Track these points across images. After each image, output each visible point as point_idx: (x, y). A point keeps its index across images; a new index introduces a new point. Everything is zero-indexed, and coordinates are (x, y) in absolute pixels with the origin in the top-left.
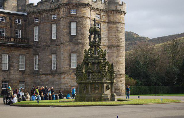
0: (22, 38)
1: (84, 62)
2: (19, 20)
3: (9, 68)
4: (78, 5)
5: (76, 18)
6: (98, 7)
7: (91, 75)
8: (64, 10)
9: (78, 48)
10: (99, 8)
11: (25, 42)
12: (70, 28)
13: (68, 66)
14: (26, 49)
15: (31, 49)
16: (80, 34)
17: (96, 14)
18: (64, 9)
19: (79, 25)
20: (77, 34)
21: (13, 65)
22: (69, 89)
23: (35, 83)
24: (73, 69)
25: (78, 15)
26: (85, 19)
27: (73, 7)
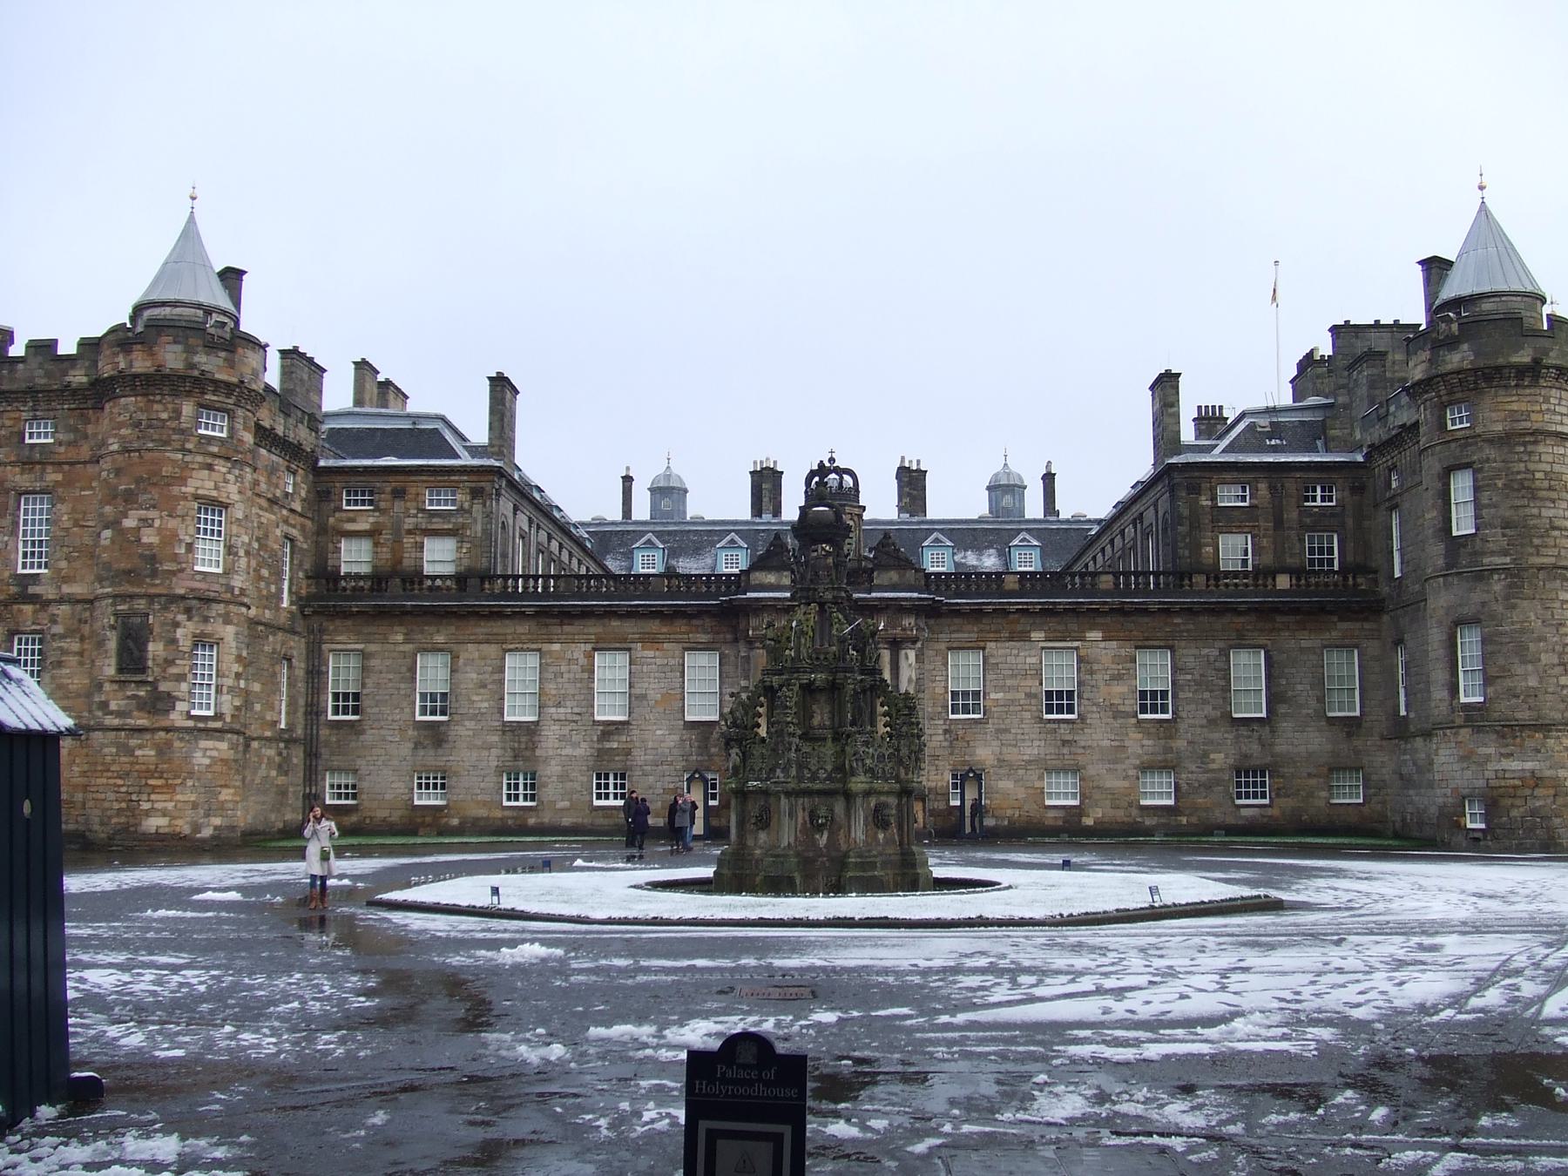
0: (1344, 570)
1: (762, 681)
2: (1323, 490)
3: (1268, 711)
5: (1467, 445)
9: (1486, 597)
11: (1308, 585)
12: (1447, 503)
13: (1445, 694)
14: (1366, 619)
15: (1386, 618)
16: (1492, 526)
19: (1483, 479)
20: (1477, 529)
21: (1290, 693)
23: (1401, 776)
25: (1479, 430)
26: (1525, 444)
27: (1450, 393)
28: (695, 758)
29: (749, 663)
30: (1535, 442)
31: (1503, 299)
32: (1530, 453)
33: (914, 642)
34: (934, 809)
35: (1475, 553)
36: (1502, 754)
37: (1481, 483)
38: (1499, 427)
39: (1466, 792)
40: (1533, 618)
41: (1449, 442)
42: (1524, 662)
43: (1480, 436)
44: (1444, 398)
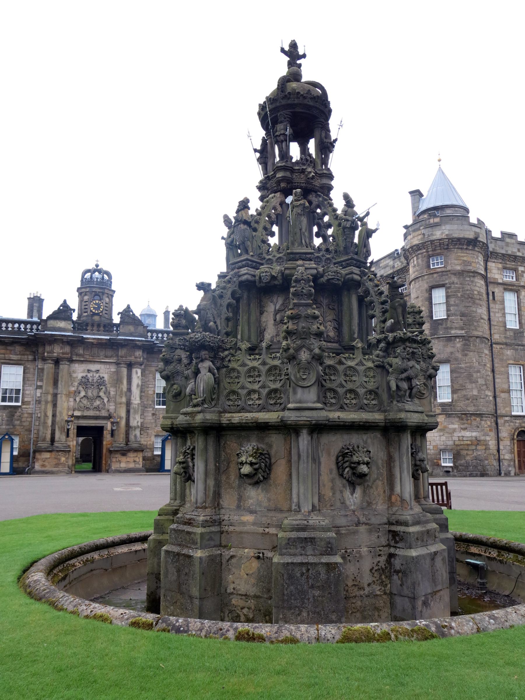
4: (448, 245)
5: (442, 275)
6: (507, 251)
7: (208, 364)
8: (415, 262)
10: (510, 252)
16: (455, 315)
17: (505, 268)
18: (415, 258)
19: (451, 292)
20: (448, 316)
22: (433, 456)
24: (443, 405)
25: (449, 268)
26: (470, 276)
28: (4, 427)
29: (43, 372)
30: (474, 277)
31: (456, 209)
32: (472, 282)
33: (141, 365)
34: (145, 457)
35: (447, 328)
36: (462, 429)
37: (450, 294)
38: (458, 268)
39: (442, 447)
40: (475, 361)
41: (433, 273)
42: (472, 382)
43: (450, 271)
44: (430, 253)
